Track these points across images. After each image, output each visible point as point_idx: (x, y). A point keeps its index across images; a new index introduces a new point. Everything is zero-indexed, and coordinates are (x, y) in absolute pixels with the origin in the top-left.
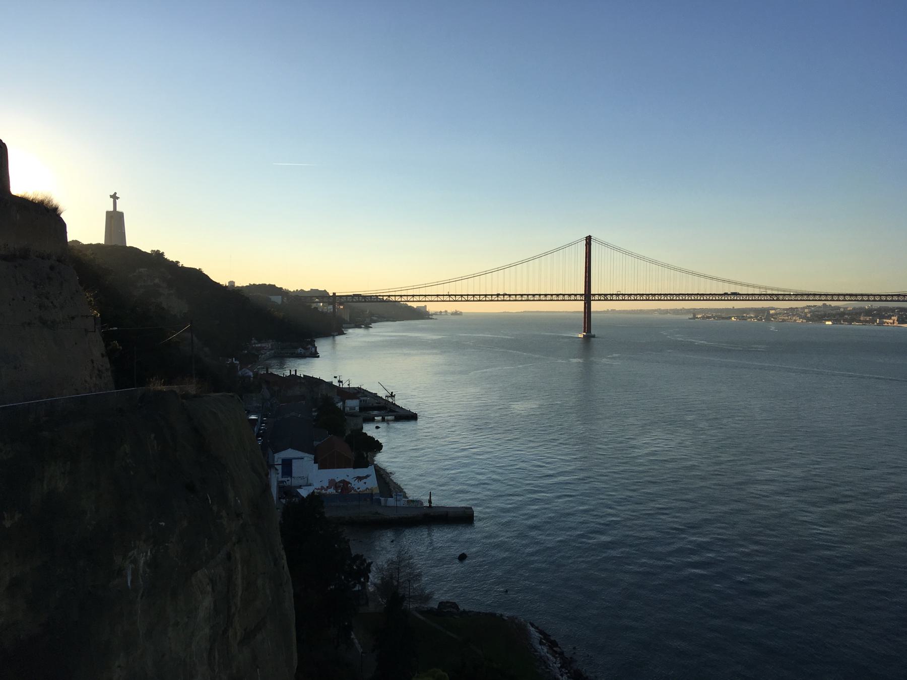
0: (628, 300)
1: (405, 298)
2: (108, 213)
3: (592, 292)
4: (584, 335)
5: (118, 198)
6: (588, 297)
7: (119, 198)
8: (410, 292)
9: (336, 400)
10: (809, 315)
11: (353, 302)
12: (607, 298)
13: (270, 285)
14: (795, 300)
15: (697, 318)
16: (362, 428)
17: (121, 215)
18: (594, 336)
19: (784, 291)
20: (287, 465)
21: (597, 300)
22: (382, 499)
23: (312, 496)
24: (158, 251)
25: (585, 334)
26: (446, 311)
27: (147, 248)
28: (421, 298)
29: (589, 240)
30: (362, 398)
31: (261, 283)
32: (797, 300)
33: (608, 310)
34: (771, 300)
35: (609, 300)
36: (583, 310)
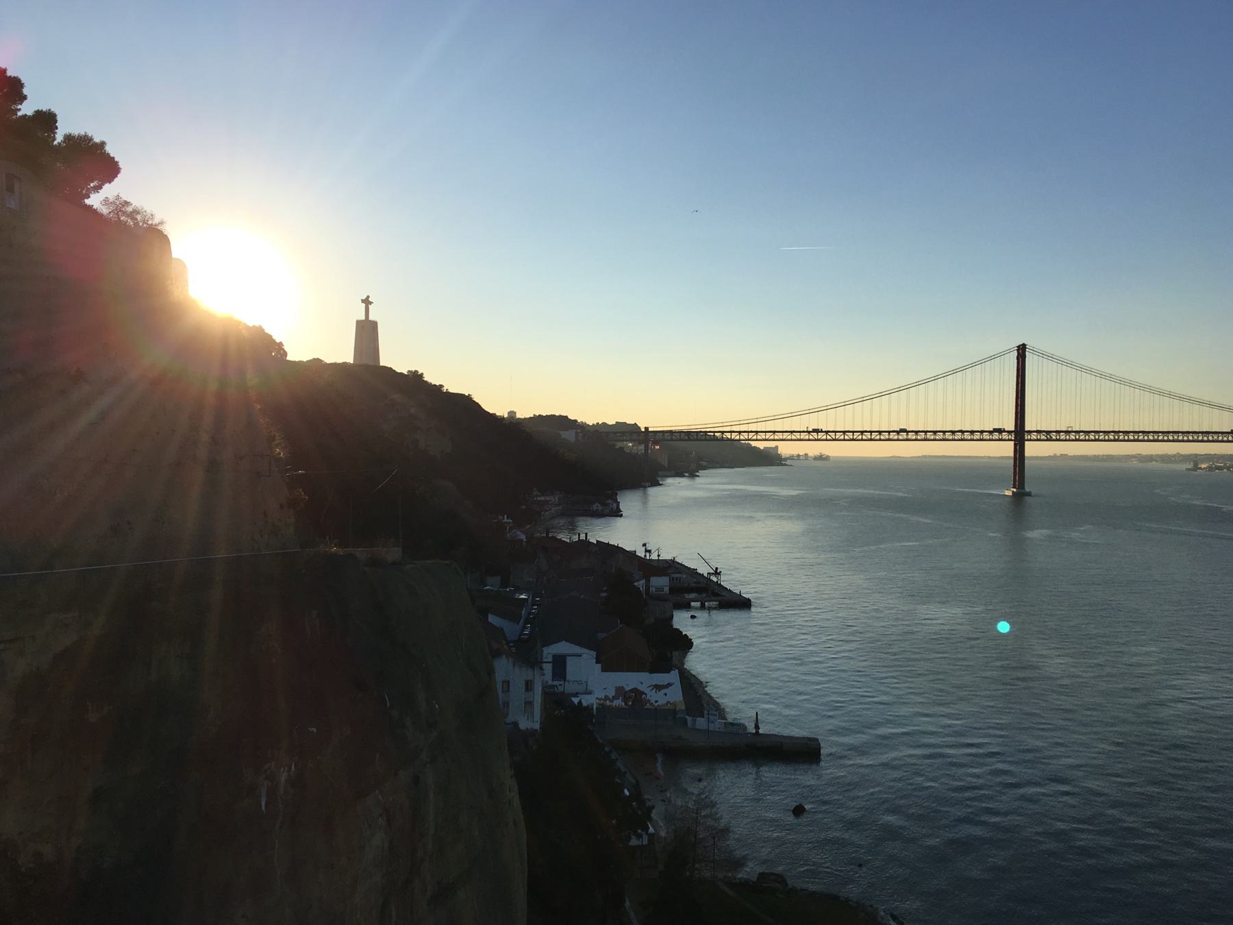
2: (358, 322)
4: (1013, 492)
5: (371, 303)
6: (1020, 434)
7: (372, 303)
8: (753, 427)
11: (672, 440)
12: (1051, 437)
13: (560, 416)
17: (374, 325)
18: (1029, 494)
21: (1035, 440)
24: (416, 371)
25: (1015, 490)
26: (806, 455)
27: (402, 368)
29: (1022, 350)
35: (1054, 440)
36: (1012, 454)
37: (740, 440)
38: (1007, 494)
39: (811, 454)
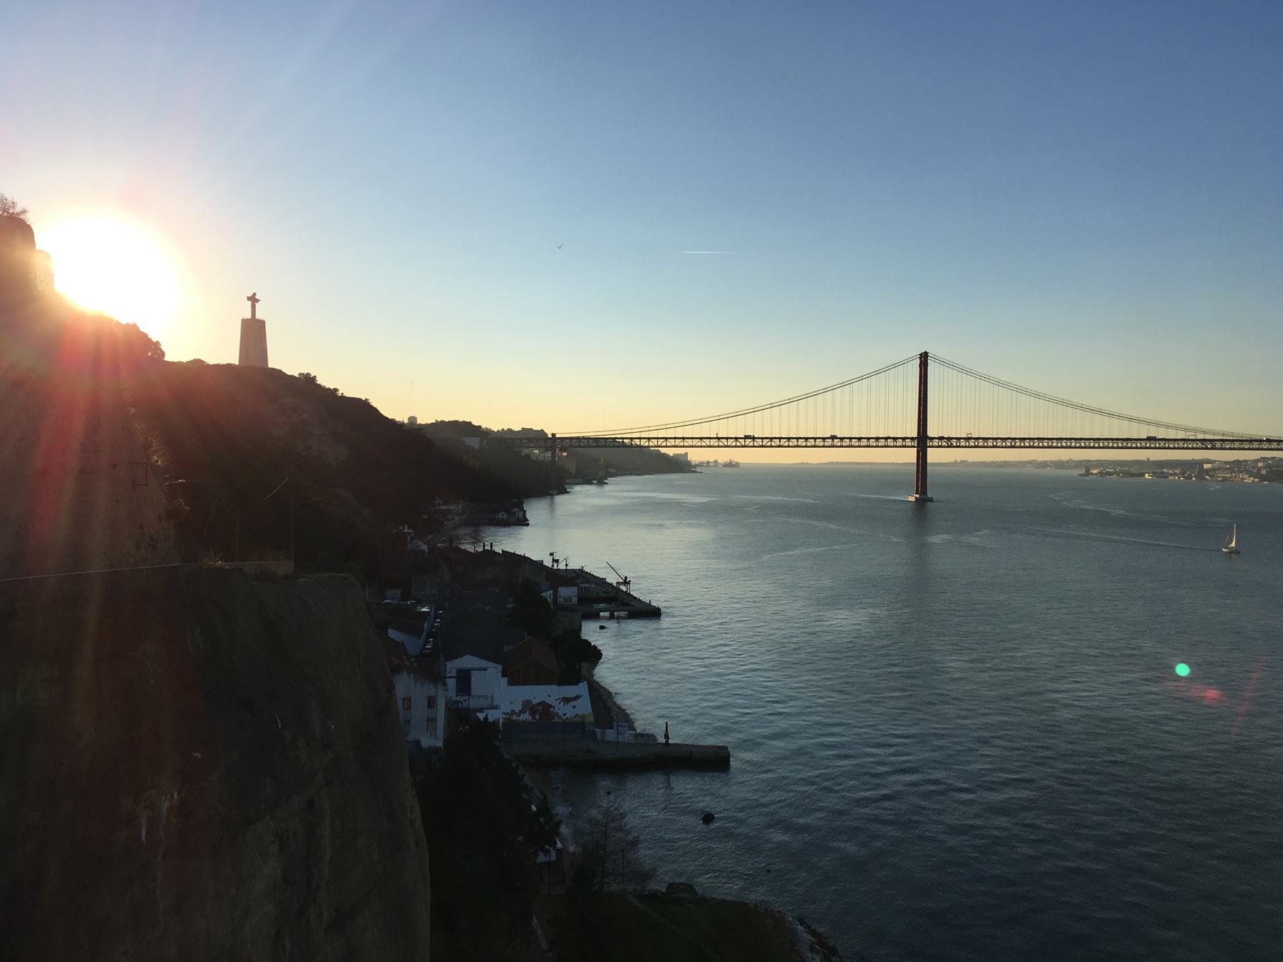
1: (654, 442)
2: (244, 321)
3: (930, 434)
4: (916, 497)
5: (258, 301)
6: (922, 441)
7: (259, 300)
10: (1263, 472)
11: (579, 446)
13: (464, 422)
14: (1239, 449)
18: (931, 500)
21: (936, 447)
24: (308, 374)
25: (918, 496)
26: (716, 461)
27: (293, 370)
29: (924, 358)
31: (452, 420)
32: (1244, 449)
33: (956, 462)
34: (1202, 449)
35: (955, 447)
36: (915, 461)
37: (649, 447)
38: (910, 500)
39: (720, 461)
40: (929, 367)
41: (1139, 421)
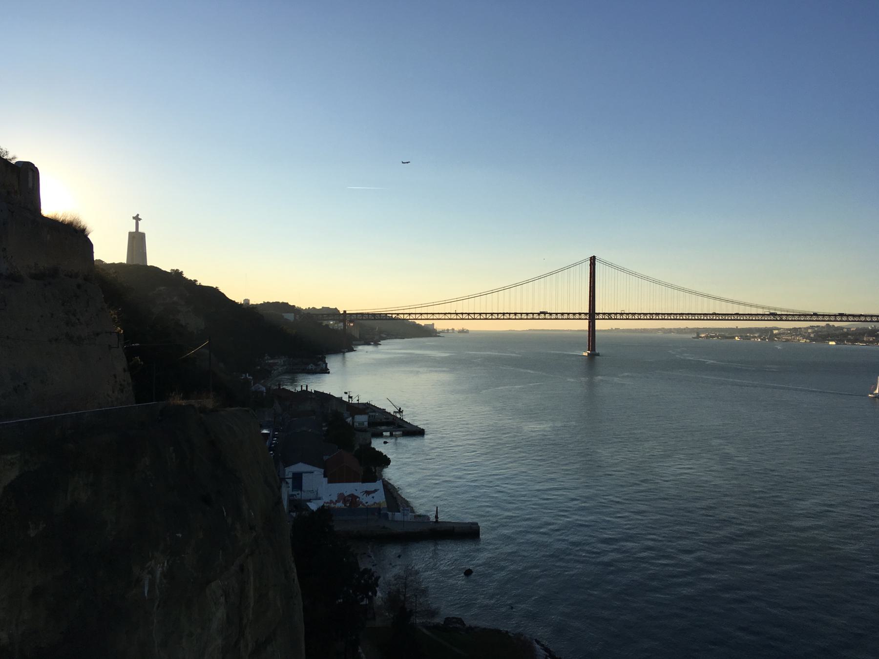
0: (632, 319)
1: (413, 316)
2: (130, 234)
4: (588, 353)
5: (140, 219)
6: (592, 316)
9: (346, 415)
10: (812, 335)
11: (362, 319)
12: (611, 317)
13: (283, 303)
14: (798, 320)
15: (701, 337)
16: (370, 443)
17: (143, 236)
18: (598, 355)
19: (787, 311)
20: (298, 479)
21: (601, 319)
22: (390, 513)
23: (322, 510)
24: (177, 270)
25: (589, 352)
26: (453, 329)
27: (167, 267)
28: (429, 316)
29: (593, 260)
30: (371, 414)
33: (612, 330)
34: (774, 320)
35: (613, 319)
36: (587, 328)
37: (410, 319)
38: (584, 354)
39: (456, 329)
40: (596, 266)
41: (733, 302)
